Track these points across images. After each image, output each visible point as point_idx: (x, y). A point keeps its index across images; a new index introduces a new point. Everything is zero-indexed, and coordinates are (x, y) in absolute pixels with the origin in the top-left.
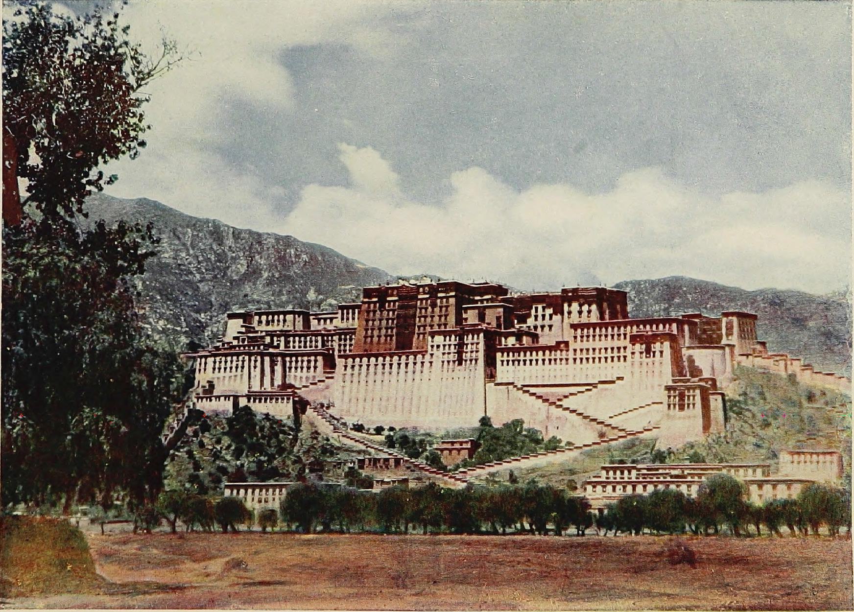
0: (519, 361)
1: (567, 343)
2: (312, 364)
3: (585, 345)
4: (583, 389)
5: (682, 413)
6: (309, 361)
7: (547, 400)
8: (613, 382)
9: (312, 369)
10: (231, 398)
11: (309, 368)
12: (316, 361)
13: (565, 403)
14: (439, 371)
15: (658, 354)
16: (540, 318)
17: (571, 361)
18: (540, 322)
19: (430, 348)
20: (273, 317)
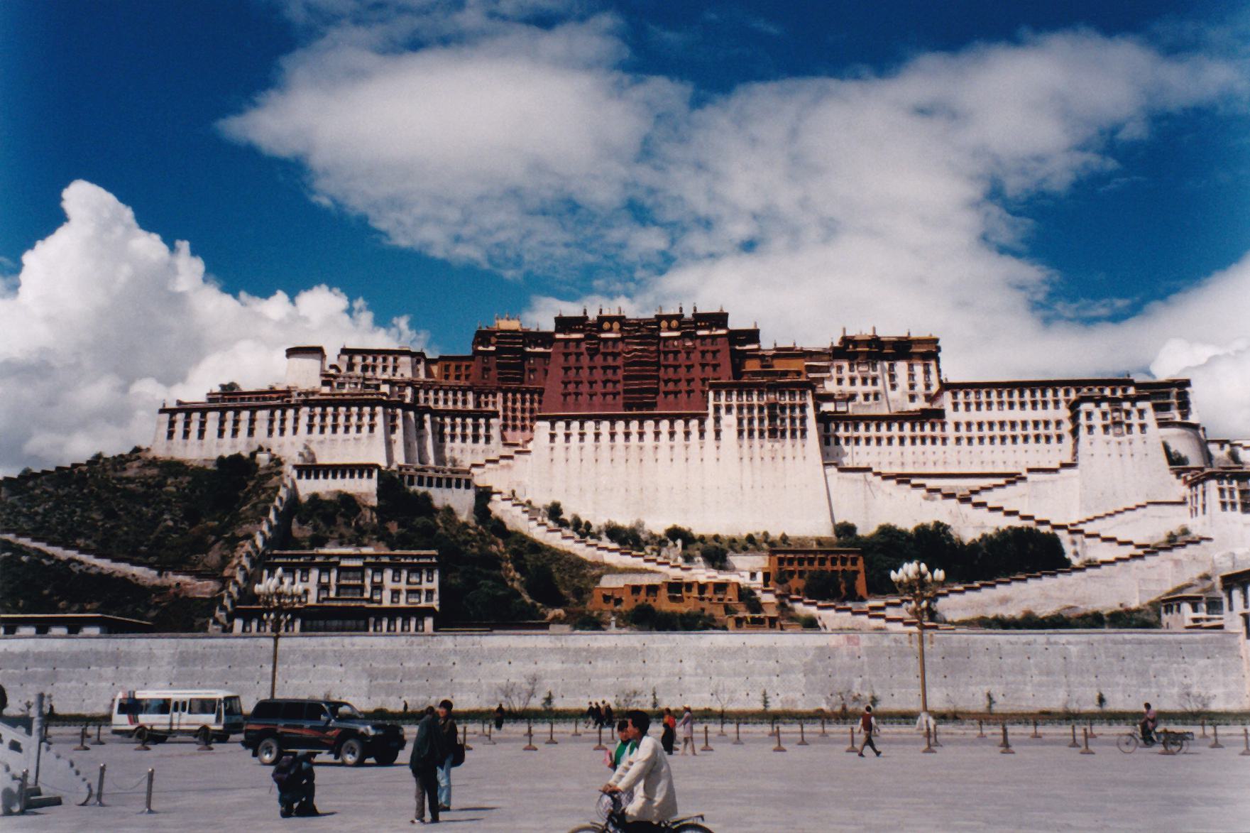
1: (940, 414)
2: (482, 431)
3: (974, 416)
4: (1002, 481)
6: (476, 427)
8: (1055, 471)
9: (482, 440)
10: (375, 474)
13: (991, 498)
14: (737, 447)
15: (1136, 429)
16: (846, 382)
18: (846, 388)
19: (711, 410)
20: (375, 360)
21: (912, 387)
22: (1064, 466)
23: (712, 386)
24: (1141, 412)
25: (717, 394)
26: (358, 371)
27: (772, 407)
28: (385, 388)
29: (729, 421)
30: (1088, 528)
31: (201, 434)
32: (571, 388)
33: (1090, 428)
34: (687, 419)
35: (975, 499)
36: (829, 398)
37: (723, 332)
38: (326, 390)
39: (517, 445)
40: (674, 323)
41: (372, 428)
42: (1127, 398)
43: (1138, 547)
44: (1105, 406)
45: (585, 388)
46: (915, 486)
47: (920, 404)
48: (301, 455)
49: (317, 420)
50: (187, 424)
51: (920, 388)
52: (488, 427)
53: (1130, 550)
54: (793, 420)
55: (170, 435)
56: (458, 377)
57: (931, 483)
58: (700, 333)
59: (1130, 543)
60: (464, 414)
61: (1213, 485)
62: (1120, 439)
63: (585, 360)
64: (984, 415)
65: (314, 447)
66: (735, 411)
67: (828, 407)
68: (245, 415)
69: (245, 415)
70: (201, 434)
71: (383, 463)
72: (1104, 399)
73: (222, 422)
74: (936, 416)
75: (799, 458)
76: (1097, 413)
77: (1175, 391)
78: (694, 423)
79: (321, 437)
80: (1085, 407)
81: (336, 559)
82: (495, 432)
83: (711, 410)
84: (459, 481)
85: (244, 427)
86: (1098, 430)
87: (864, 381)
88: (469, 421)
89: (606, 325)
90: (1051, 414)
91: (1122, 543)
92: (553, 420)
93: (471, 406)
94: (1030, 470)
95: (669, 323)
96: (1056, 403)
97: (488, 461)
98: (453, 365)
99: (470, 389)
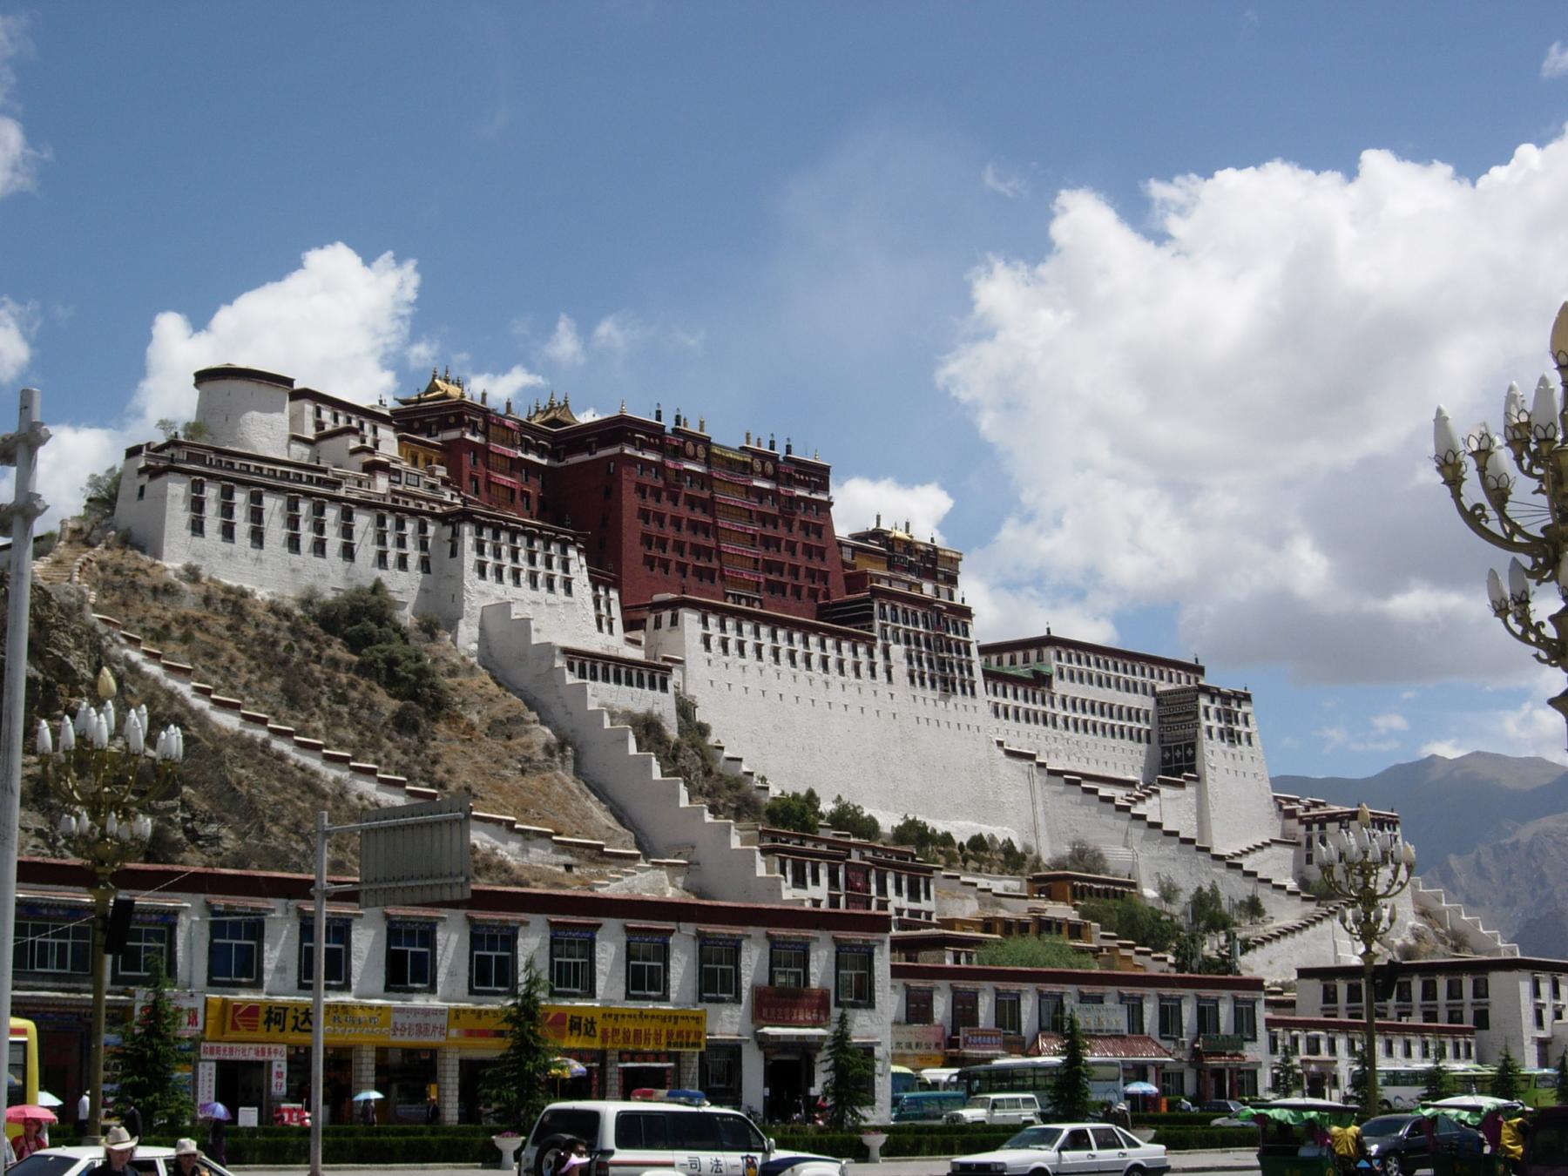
25: (882, 606)
31: (257, 537)
40: (769, 467)
44: (1218, 704)
55: (197, 528)
57: (1104, 791)
58: (800, 492)
62: (1232, 750)
63: (666, 507)
70: (257, 537)
74: (1041, 681)
78: (861, 650)
80: (1204, 701)
89: (690, 447)
92: (705, 610)
95: (763, 463)
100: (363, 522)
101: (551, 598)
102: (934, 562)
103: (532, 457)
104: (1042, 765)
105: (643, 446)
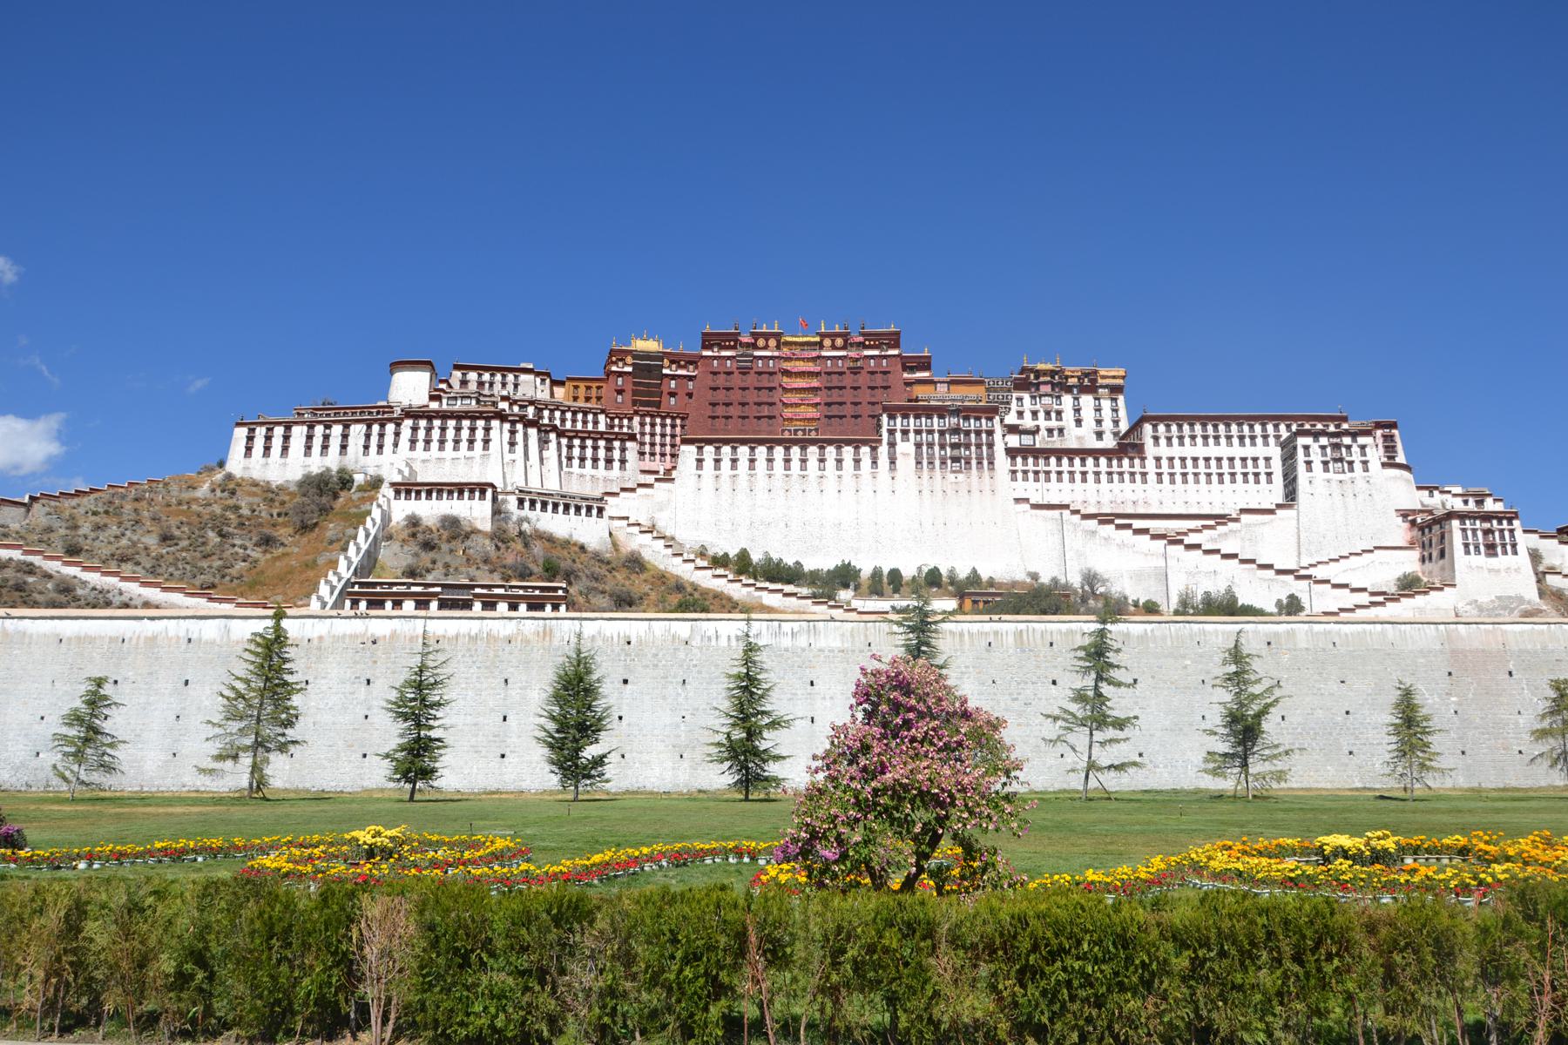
0: (1048, 473)
2: (616, 454)
3: (1176, 451)
4: (1212, 523)
5: (1492, 560)
6: (609, 449)
7: (1163, 537)
8: (1271, 512)
9: (616, 464)
11: (609, 461)
12: (623, 450)
14: (913, 477)
16: (1028, 415)
17: (1152, 477)
18: (1028, 422)
19: (885, 436)
21: (1099, 422)
22: (1279, 506)
23: (885, 409)
24: (1363, 447)
25: (892, 417)
26: (473, 387)
27: (956, 431)
28: (504, 405)
29: (906, 448)
30: (1319, 572)
31: (285, 449)
32: (720, 411)
33: (1309, 469)
34: (857, 444)
35: (1187, 541)
36: (1013, 429)
37: (896, 352)
38: (434, 405)
39: (657, 472)
40: (839, 342)
41: (486, 442)
42: (1347, 433)
43: (1373, 594)
44: (1324, 441)
45: (734, 411)
46: (1119, 527)
47: (1109, 442)
48: (400, 472)
49: (421, 434)
50: (268, 438)
51: (1108, 425)
52: (623, 450)
53: (1364, 598)
54: (979, 446)
56: (588, 399)
57: (1138, 524)
59: (1364, 590)
60: (596, 436)
61: (1455, 523)
62: (1341, 477)
63: (737, 380)
64: (1188, 451)
65: (417, 466)
66: (912, 435)
67: (1014, 441)
68: (337, 430)
69: (337, 430)
70: (285, 449)
71: (499, 485)
72: (1324, 433)
73: (310, 437)
75: (987, 492)
76: (1315, 448)
77: (1379, 433)
78: (865, 450)
79: (426, 455)
80: (1301, 441)
81: (438, 589)
82: (632, 455)
83: (885, 436)
84: (589, 509)
85: (335, 443)
86: (1317, 466)
87: (1048, 413)
88: (602, 443)
89: (761, 342)
90: (1260, 450)
91: (1354, 590)
92: (700, 443)
93: (602, 427)
94: (1243, 511)
96: (1265, 437)
97: (623, 490)
98: (582, 385)
99: (603, 411)
100: (357, 430)
101: (470, 454)
102: (1094, 381)
103: (680, 372)
104: (1077, 512)
105: (722, 348)
